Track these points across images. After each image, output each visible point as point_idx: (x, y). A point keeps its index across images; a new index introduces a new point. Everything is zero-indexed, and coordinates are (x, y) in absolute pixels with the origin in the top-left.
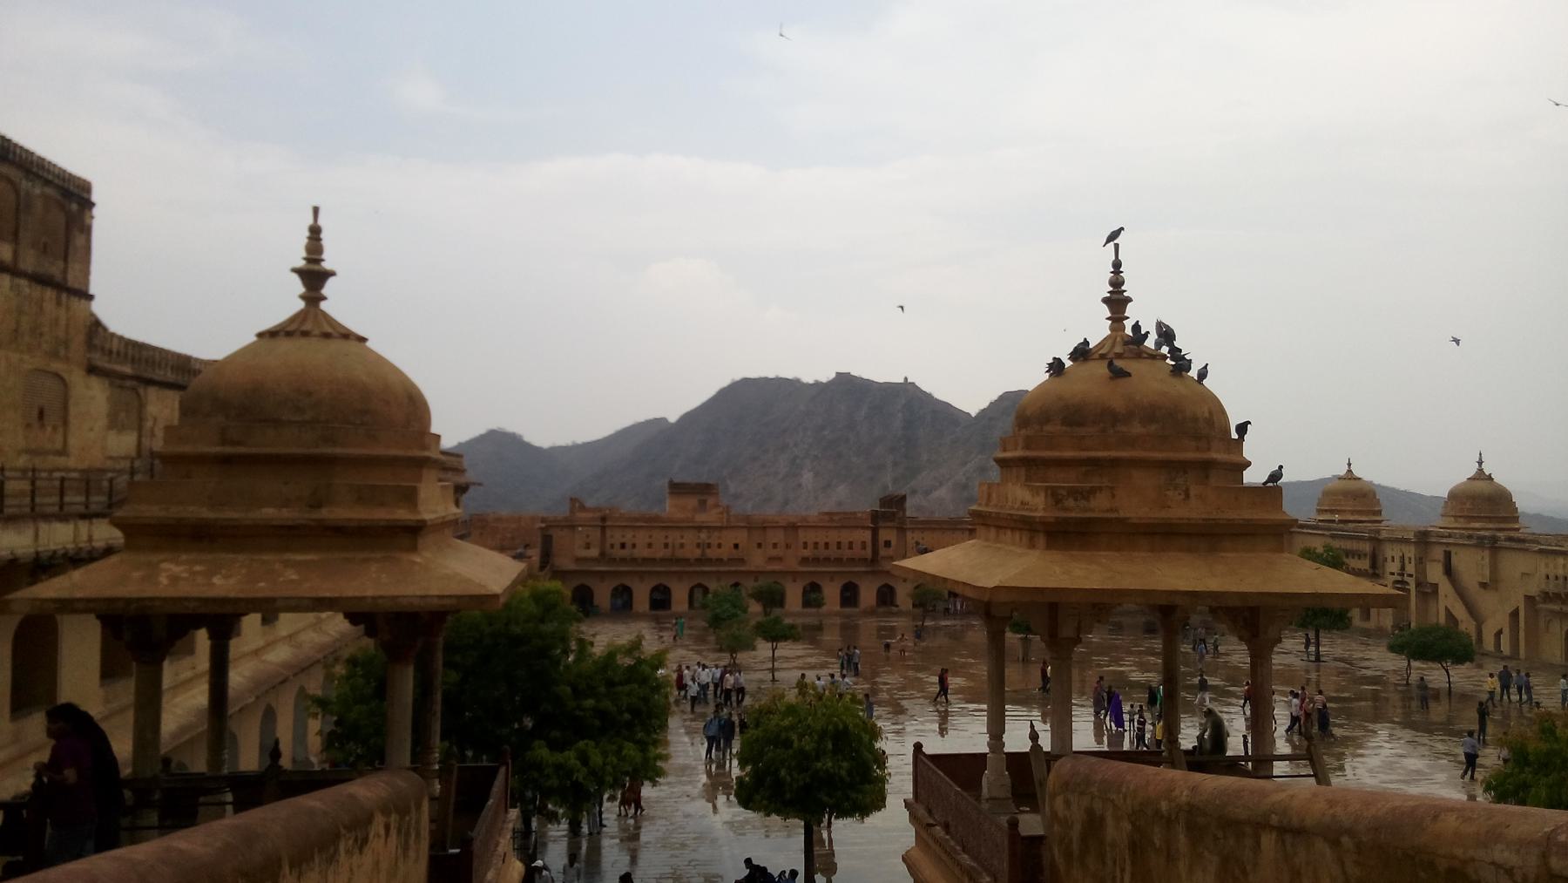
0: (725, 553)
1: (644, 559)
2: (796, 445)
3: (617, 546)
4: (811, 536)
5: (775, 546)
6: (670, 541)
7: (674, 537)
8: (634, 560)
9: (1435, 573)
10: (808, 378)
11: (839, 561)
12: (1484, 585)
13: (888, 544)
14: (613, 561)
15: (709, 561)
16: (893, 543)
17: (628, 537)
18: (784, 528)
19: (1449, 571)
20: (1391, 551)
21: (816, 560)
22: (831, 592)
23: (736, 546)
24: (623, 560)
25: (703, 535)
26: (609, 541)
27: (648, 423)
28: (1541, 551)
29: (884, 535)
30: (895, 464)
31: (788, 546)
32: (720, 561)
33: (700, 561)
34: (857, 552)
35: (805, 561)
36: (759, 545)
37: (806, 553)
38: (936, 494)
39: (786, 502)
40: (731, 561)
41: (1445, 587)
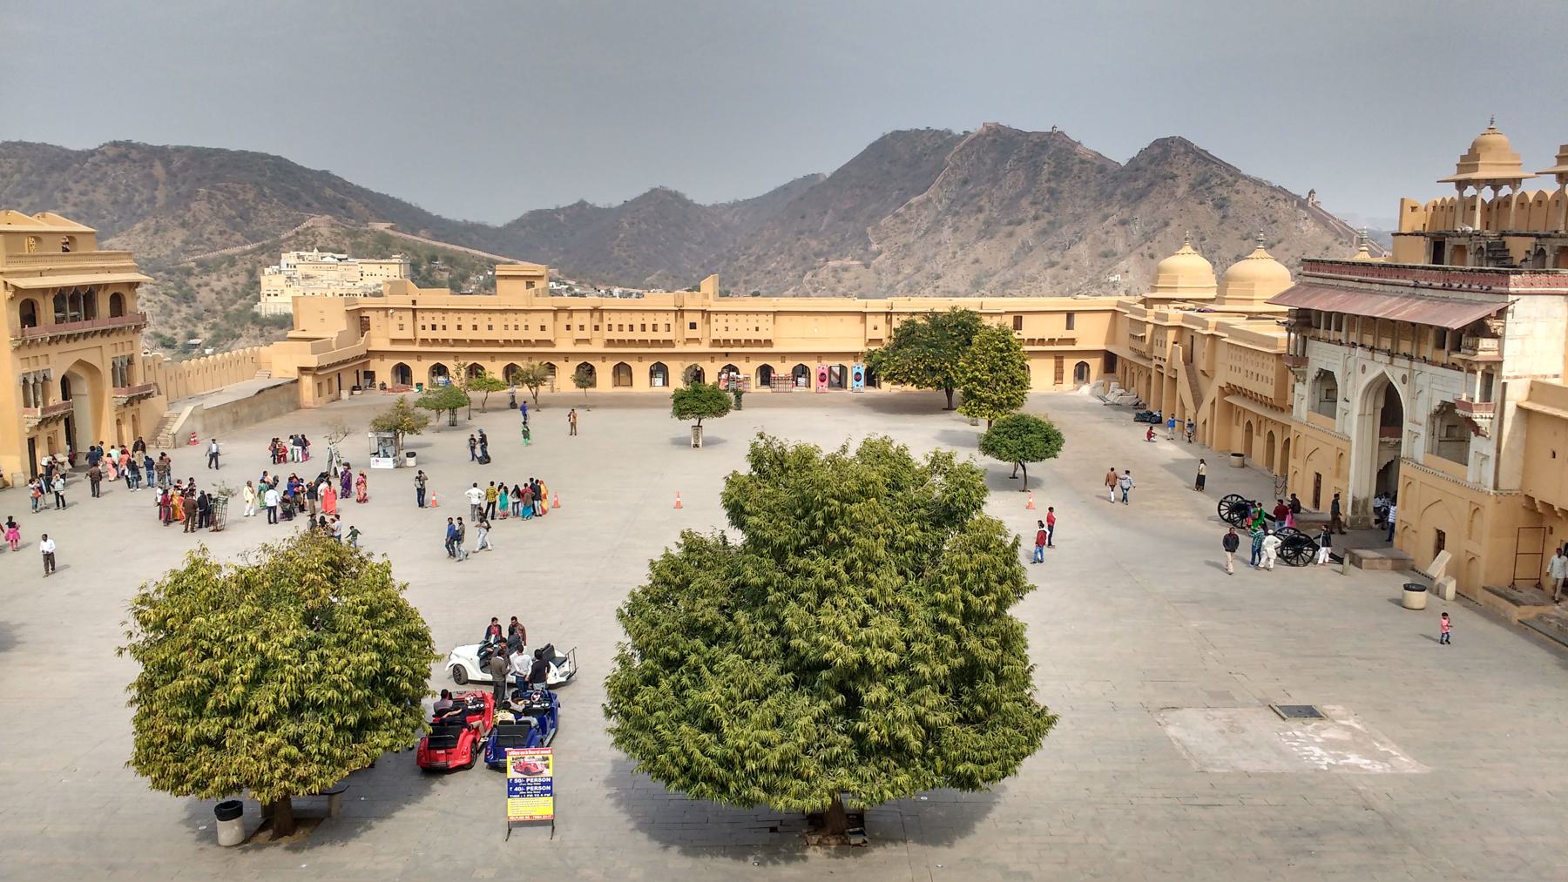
3: (429, 327)
8: (445, 341)
11: (643, 343)
13: (693, 326)
14: (424, 341)
15: (517, 342)
17: (438, 319)
21: (621, 342)
22: (641, 370)
23: (543, 328)
24: (435, 341)
26: (420, 323)
31: (597, 328)
32: (527, 342)
33: (507, 342)
35: (610, 342)
36: (568, 327)
40: (539, 342)
41: (1182, 377)
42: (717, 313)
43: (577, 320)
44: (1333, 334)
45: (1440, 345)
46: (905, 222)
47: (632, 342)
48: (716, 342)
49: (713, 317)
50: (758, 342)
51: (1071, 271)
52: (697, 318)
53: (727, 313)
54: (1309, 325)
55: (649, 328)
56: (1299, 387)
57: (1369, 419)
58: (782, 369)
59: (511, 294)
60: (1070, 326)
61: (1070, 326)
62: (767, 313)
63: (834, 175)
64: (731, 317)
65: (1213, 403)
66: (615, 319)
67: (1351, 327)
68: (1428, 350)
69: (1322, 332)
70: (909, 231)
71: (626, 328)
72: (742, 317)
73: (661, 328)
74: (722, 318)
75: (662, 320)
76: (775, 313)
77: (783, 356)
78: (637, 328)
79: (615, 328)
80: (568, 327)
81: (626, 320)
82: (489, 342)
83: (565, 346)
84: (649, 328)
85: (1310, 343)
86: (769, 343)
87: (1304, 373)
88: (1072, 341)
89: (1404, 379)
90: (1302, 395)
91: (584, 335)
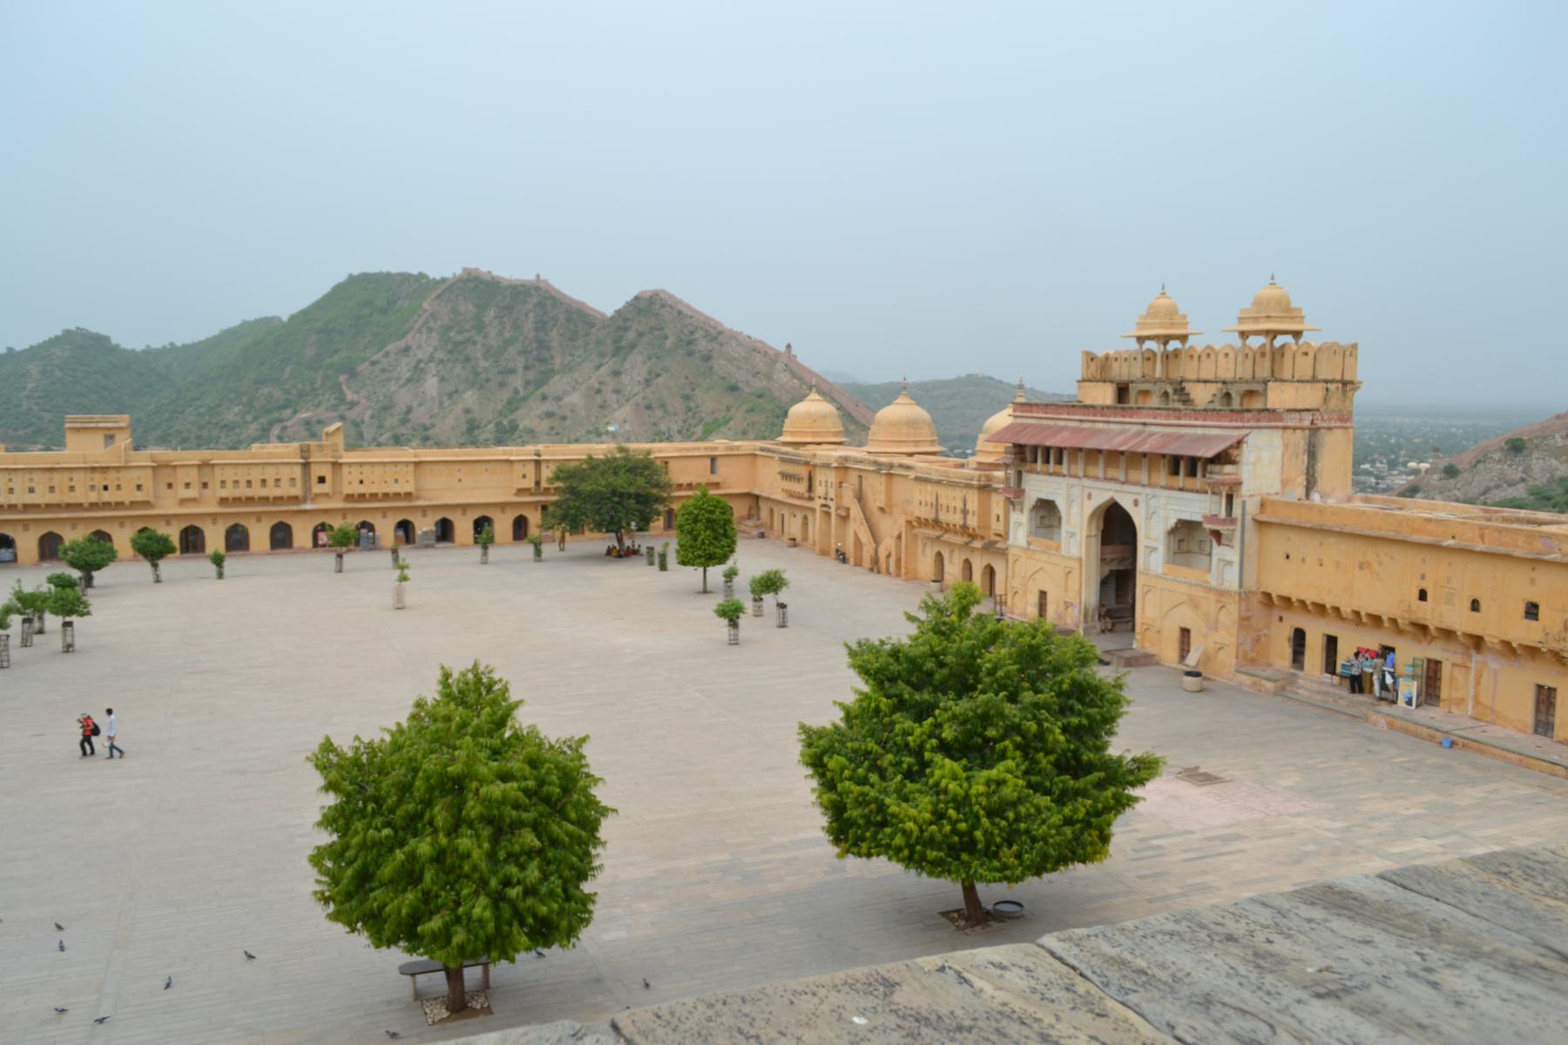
0: (126, 496)
1: (48, 506)
2: (419, 347)
4: (229, 475)
5: (187, 485)
6: (55, 483)
7: (59, 480)
9: (849, 499)
10: (435, 273)
11: (264, 500)
12: (882, 510)
13: (322, 480)
15: (106, 505)
16: (328, 479)
18: (199, 466)
19: (860, 497)
20: (820, 476)
21: (237, 501)
23: (139, 487)
25: (99, 480)
27: (259, 322)
28: (917, 479)
29: (316, 472)
30: (526, 368)
31: (205, 485)
32: (119, 505)
33: (94, 506)
34: (285, 490)
36: (170, 486)
37: (224, 493)
38: (567, 400)
39: (409, 410)
40: (133, 505)
41: (855, 511)
42: (350, 464)
43: (182, 477)
44: (1052, 467)
45: (1175, 472)
46: (383, 371)
47: (250, 500)
48: (349, 497)
49: (345, 470)
50: (397, 496)
51: (568, 422)
52: (326, 471)
53: (361, 464)
54: (1023, 460)
55: (271, 483)
56: (1015, 517)
57: (1094, 540)
58: (425, 525)
59: (82, 448)
60: (713, 471)
61: (713, 471)
62: (407, 463)
63: (292, 318)
64: (366, 470)
65: (899, 537)
66: (229, 475)
67: (1073, 460)
68: (1162, 477)
69: (1039, 465)
70: (389, 380)
71: (243, 483)
72: (378, 470)
73: (285, 483)
74: (355, 471)
75: (285, 474)
76: (417, 464)
77: (424, 510)
78: (256, 483)
79: (229, 484)
80: (170, 486)
81: (242, 475)
82: (69, 507)
83: (168, 506)
84: (271, 483)
85: (1026, 476)
86: (409, 495)
87: (1021, 504)
88: (717, 485)
89: (1136, 503)
90: (1020, 526)
91: (192, 493)
